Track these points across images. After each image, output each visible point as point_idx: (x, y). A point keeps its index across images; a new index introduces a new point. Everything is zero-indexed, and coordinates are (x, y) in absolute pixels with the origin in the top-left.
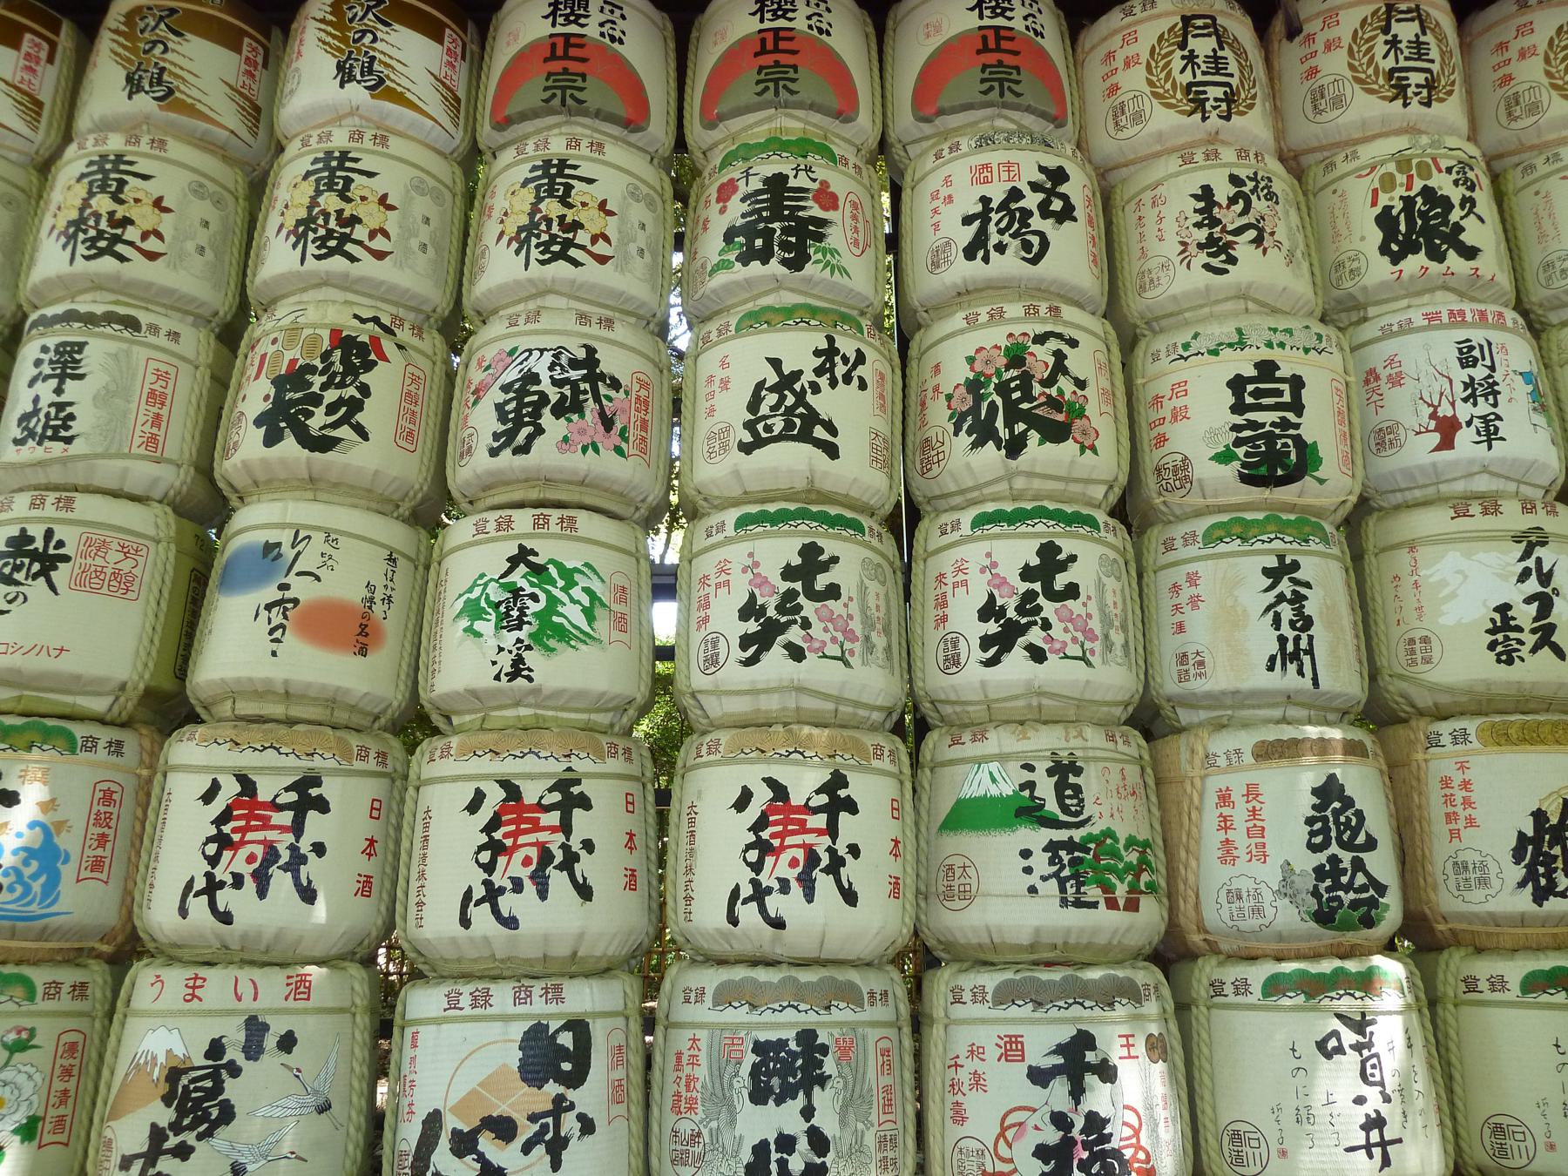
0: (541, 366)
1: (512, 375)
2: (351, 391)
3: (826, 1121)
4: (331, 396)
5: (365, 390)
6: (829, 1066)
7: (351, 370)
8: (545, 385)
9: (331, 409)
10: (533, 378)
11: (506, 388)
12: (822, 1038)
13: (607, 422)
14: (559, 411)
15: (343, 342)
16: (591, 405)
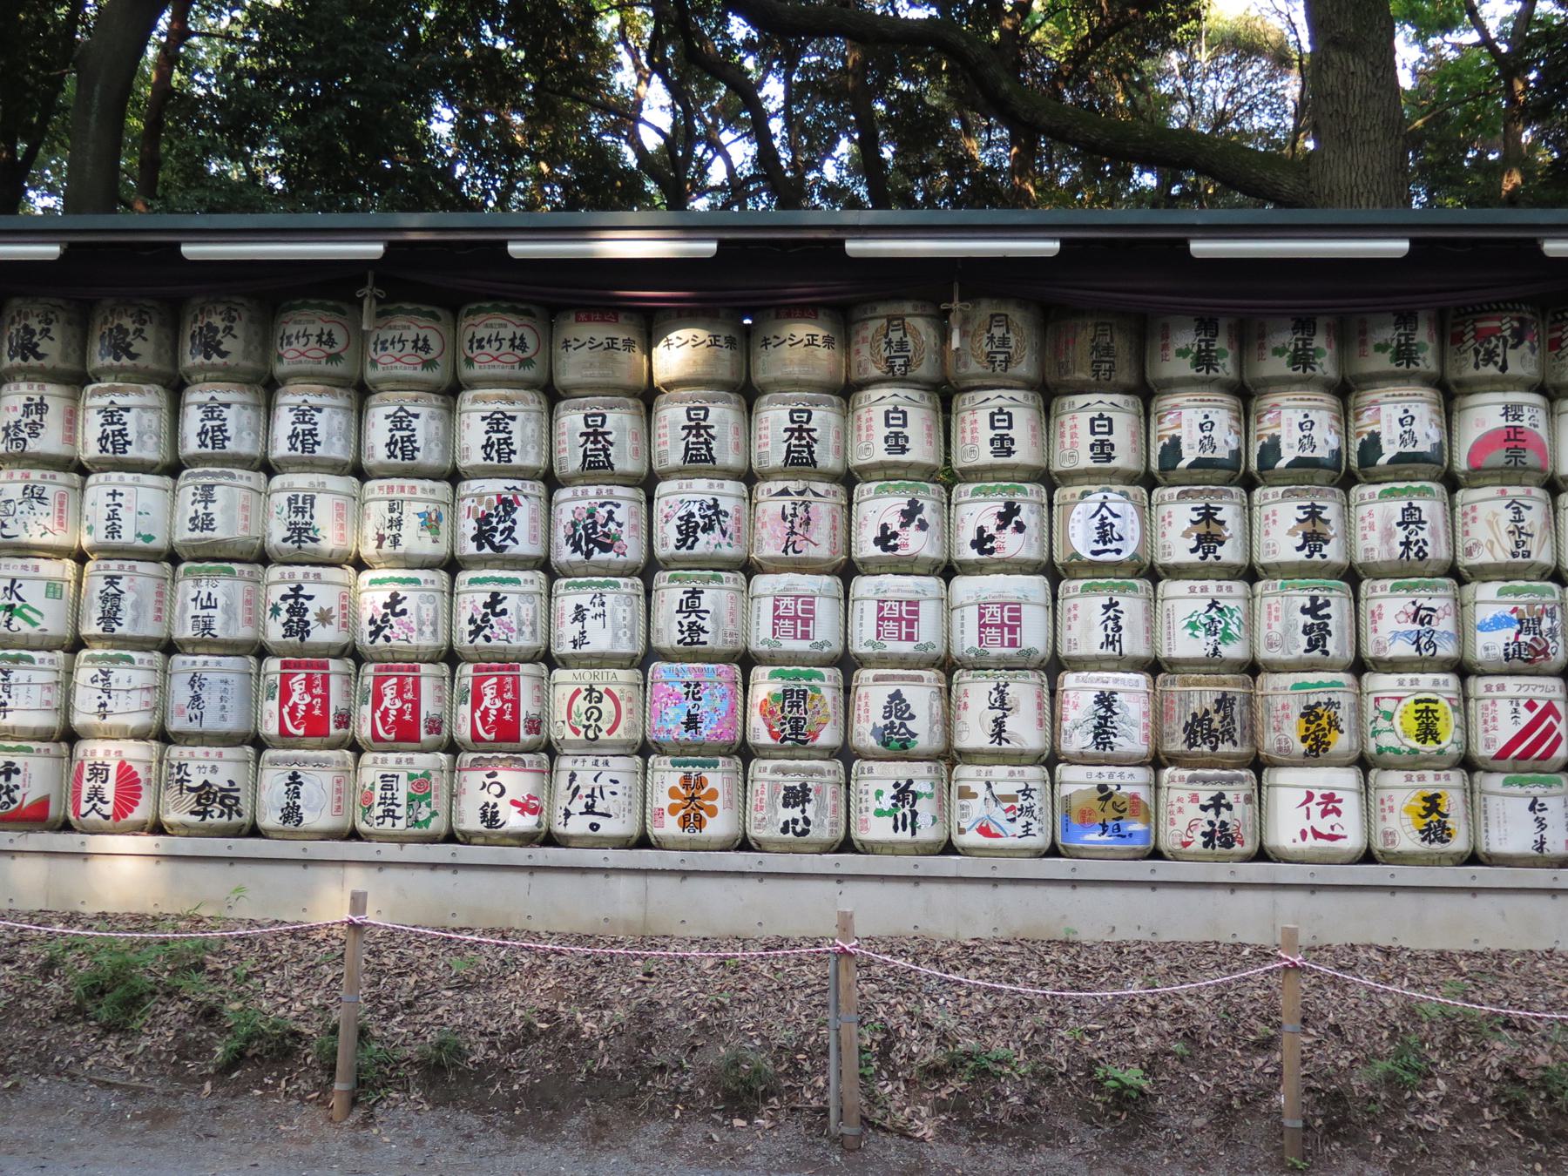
0: (695, 509)
1: (683, 513)
2: (509, 523)
3: (810, 814)
4: (501, 527)
5: (514, 522)
6: (812, 796)
7: (507, 513)
8: (698, 519)
9: (502, 533)
10: (691, 515)
11: (681, 519)
12: (809, 785)
13: (724, 533)
14: (704, 530)
15: (503, 501)
16: (717, 527)
